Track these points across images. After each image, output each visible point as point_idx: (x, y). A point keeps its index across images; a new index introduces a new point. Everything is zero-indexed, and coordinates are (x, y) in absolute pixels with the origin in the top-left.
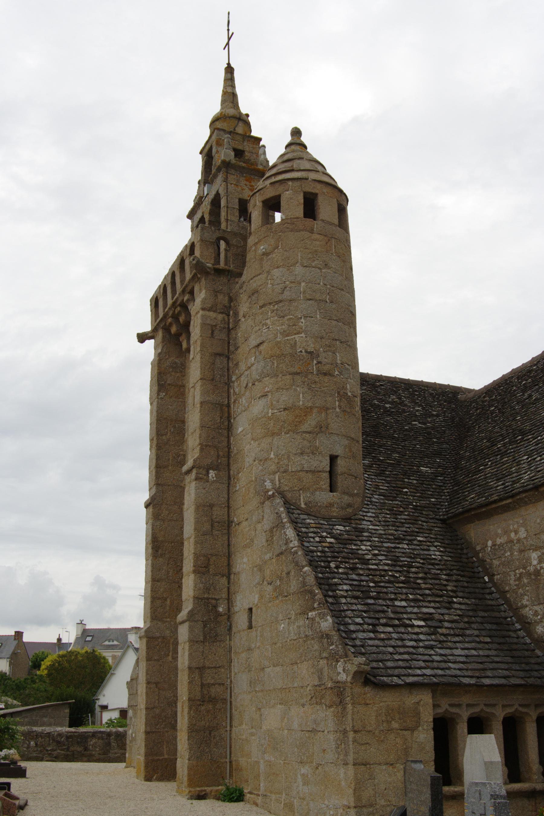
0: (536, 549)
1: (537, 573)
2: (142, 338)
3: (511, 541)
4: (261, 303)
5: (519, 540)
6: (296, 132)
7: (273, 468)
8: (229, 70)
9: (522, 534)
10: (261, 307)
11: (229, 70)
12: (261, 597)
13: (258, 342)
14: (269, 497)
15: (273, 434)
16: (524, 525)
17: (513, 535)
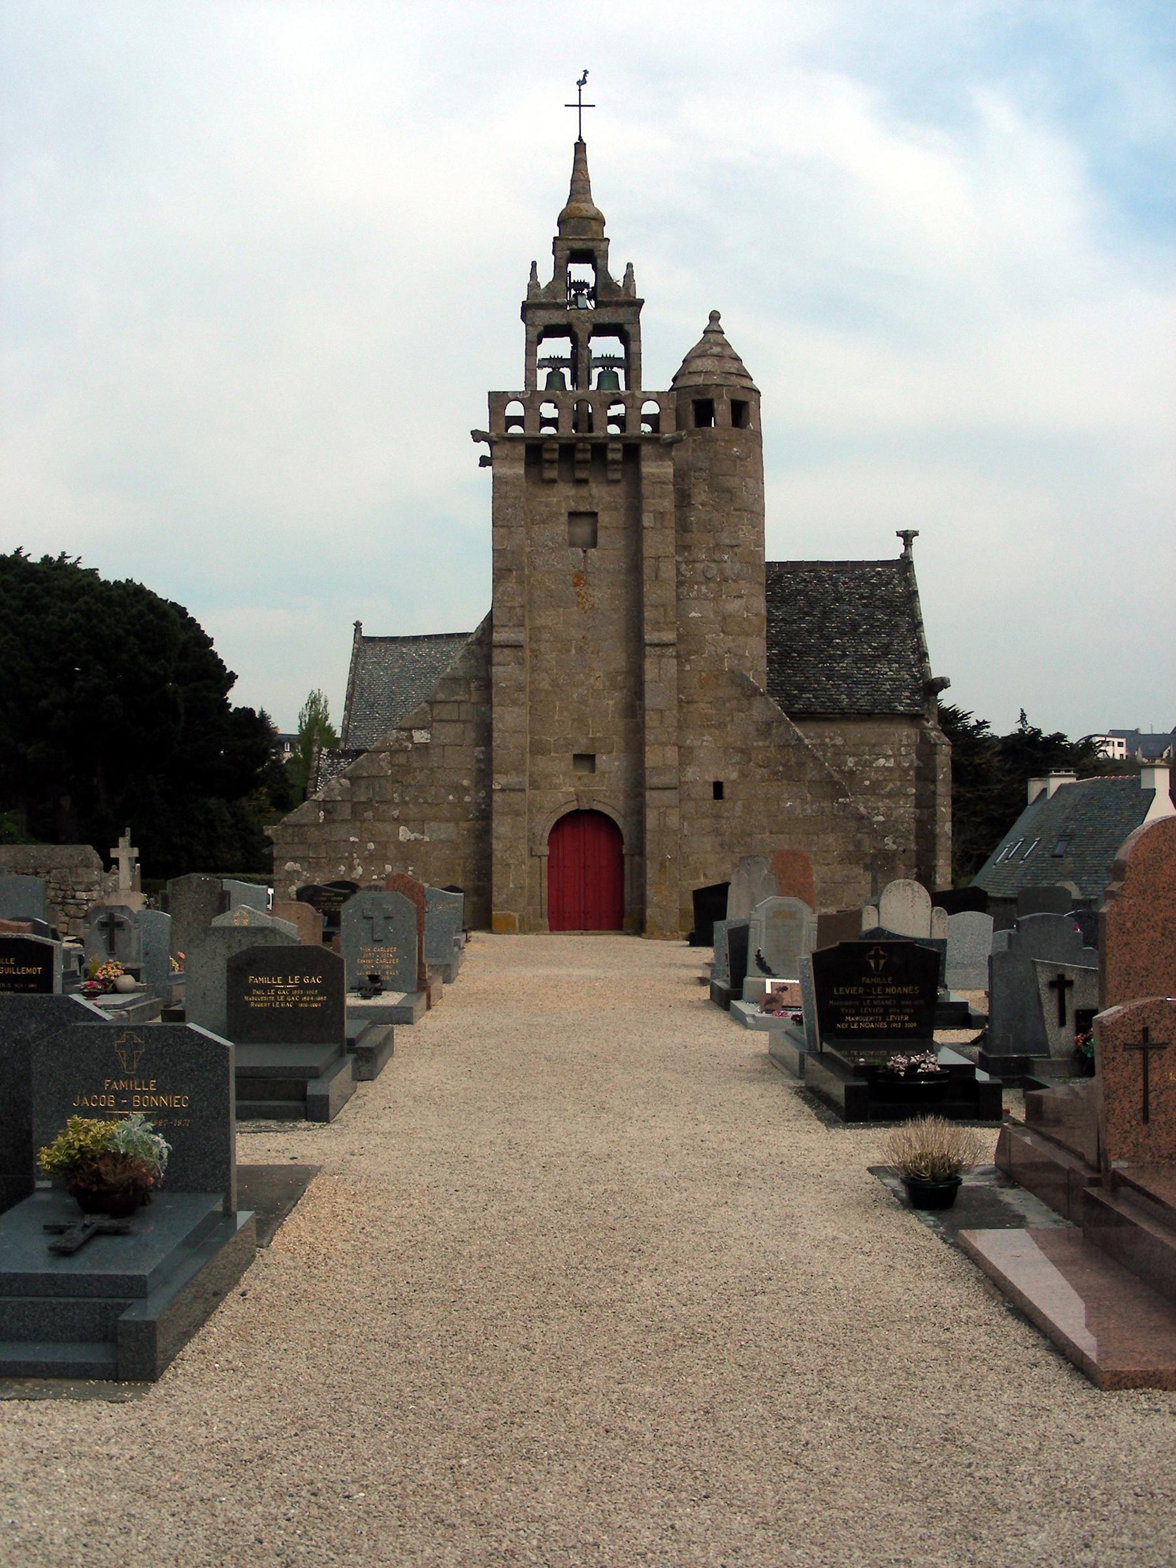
0: (854, 755)
1: (852, 773)
2: (477, 436)
3: (826, 745)
4: (737, 506)
5: (834, 746)
6: (714, 317)
7: (749, 665)
8: (580, 147)
9: (839, 741)
10: (735, 510)
11: (580, 147)
12: (743, 775)
13: (734, 543)
14: (762, 695)
15: (748, 635)
16: (843, 735)
17: (827, 740)
